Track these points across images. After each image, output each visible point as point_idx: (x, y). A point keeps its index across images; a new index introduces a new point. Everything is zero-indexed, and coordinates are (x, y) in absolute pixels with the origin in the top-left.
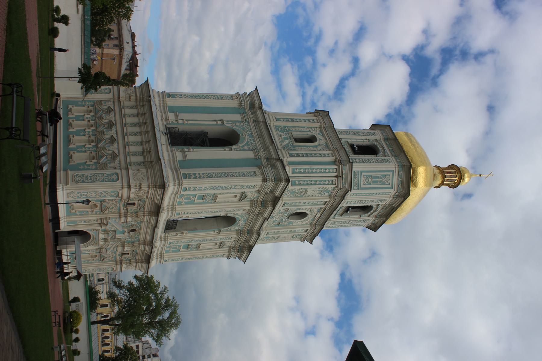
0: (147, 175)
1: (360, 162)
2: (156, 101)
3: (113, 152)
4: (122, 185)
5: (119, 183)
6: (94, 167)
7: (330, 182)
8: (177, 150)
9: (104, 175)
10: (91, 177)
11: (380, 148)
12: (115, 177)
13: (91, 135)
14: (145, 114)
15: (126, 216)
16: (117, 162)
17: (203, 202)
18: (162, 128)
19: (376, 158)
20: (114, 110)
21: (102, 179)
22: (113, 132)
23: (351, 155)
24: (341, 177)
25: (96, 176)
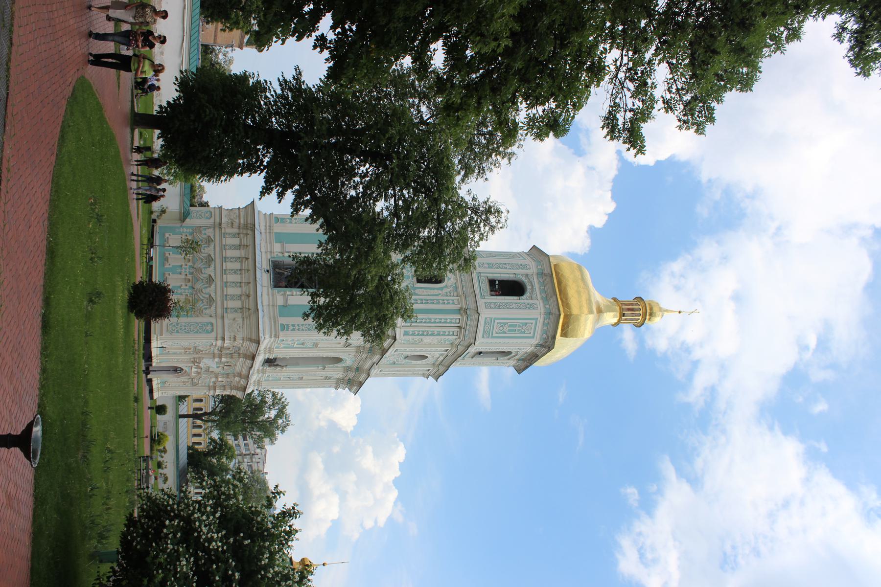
0: (243, 327)
1: (495, 308)
2: (260, 225)
3: (210, 296)
4: (217, 337)
5: (213, 334)
7: (451, 333)
8: (278, 293)
10: (185, 326)
11: (529, 287)
12: (209, 328)
13: (188, 274)
14: (247, 246)
15: (220, 357)
16: (213, 308)
19: (518, 301)
21: (196, 330)
22: (210, 271)
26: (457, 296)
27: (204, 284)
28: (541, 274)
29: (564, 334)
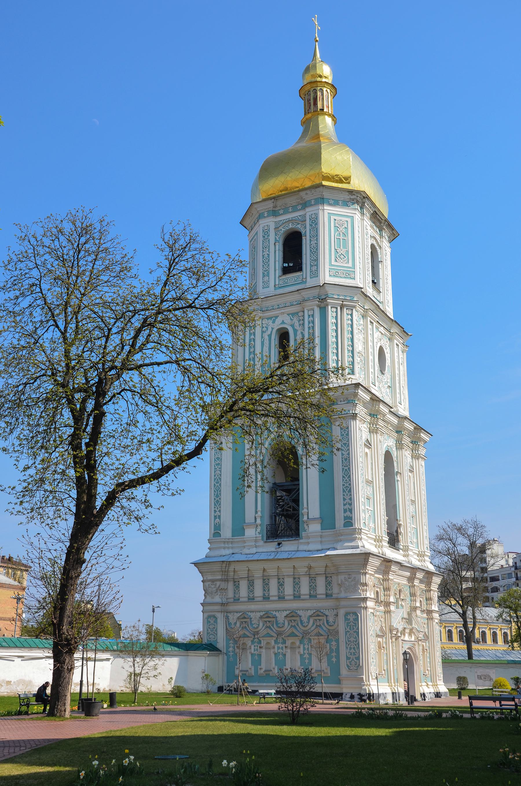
1: (317, 265)
3: (311, 616)
6: (334, 643)
9: (348, 632)
10: (351, 648)
11: (291, 226)
16: (327, 613)
17: (372, 499)
18: (272, 546)
20: (244, 613)
22: (281, 617)
23: (303, 275)
24: (343, 302)
25: (349, 641)
26: (303, 312)
27: (298, 625)
28: (274, 213)
29: (347, 179)
